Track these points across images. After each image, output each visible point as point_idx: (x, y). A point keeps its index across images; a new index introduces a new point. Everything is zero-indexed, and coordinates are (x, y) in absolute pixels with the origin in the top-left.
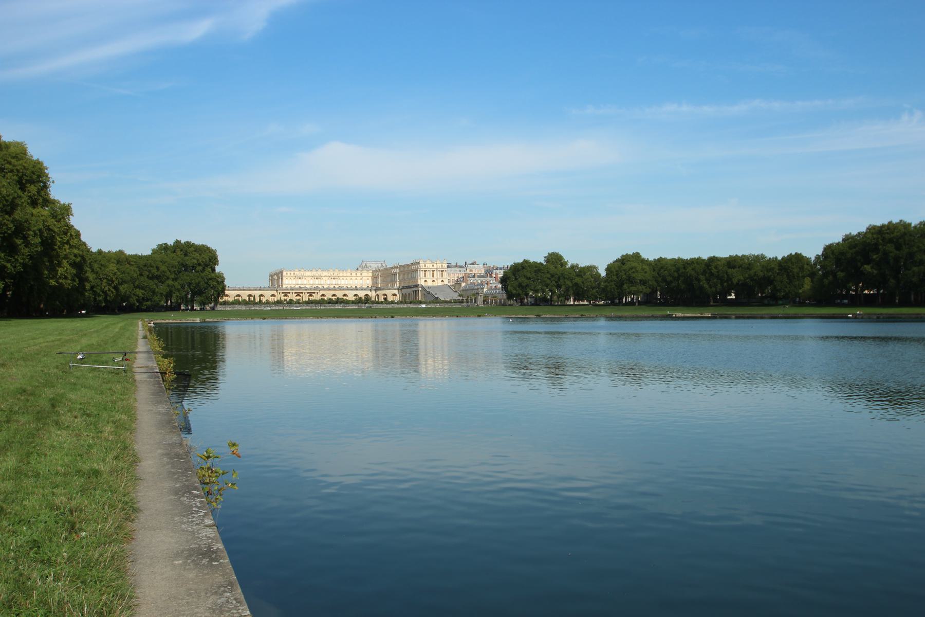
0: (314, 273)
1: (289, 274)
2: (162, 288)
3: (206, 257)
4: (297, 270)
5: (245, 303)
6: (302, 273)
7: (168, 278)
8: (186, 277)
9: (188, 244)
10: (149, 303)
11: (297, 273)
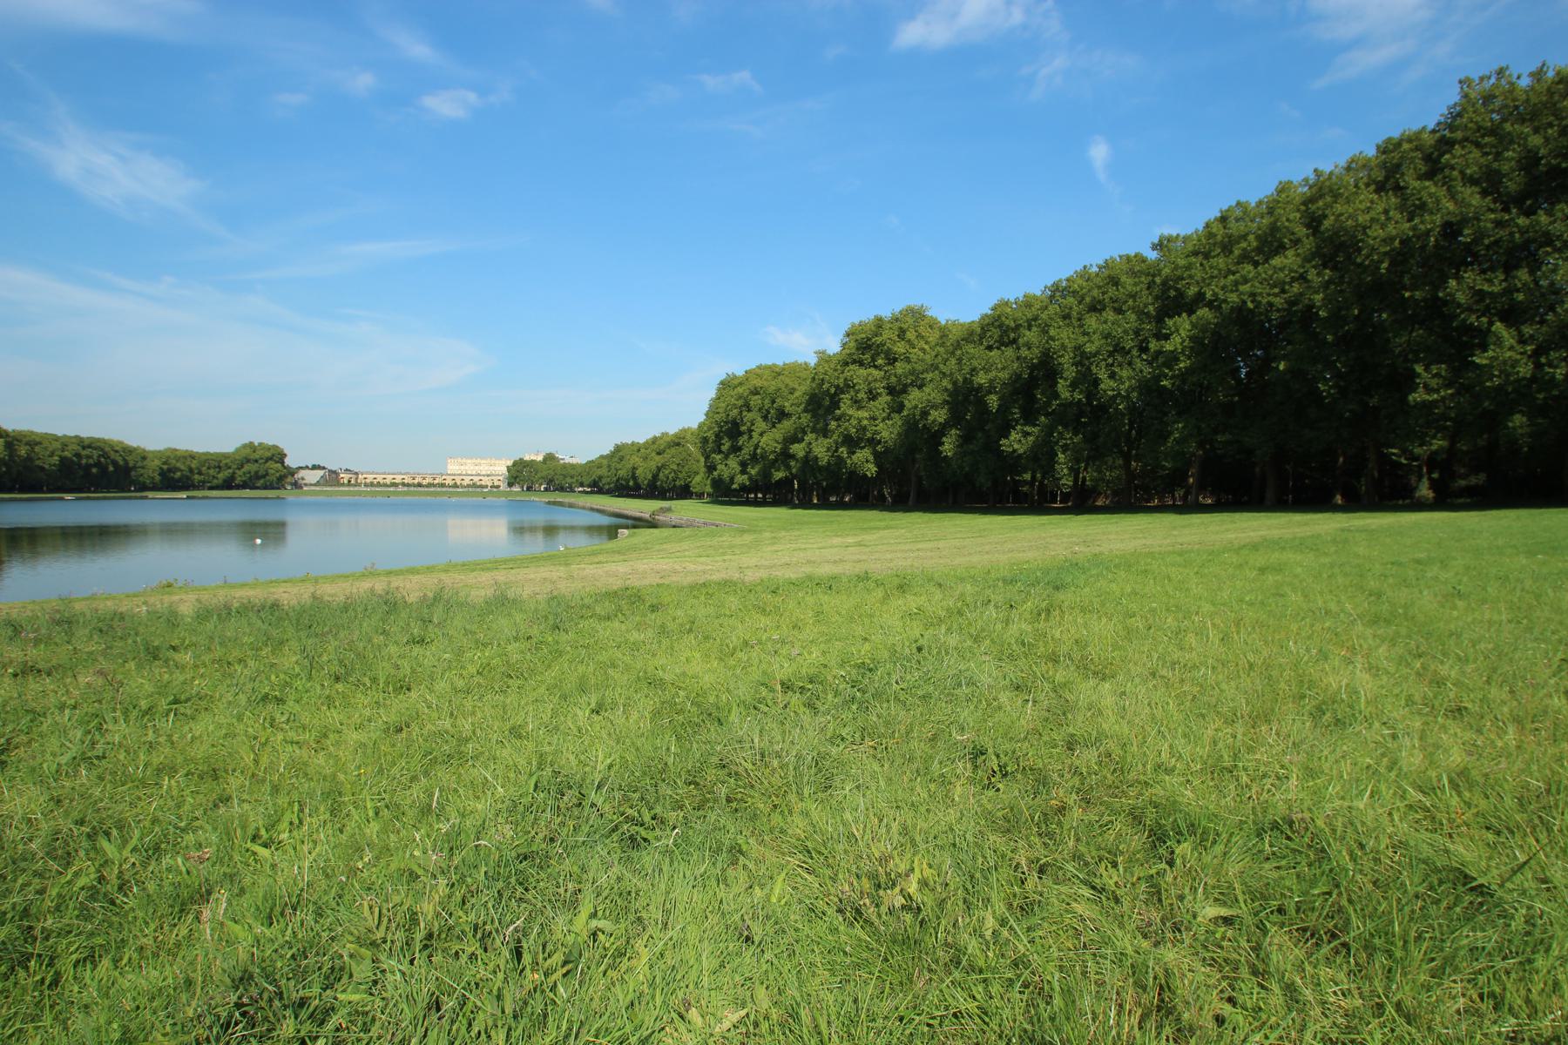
0: (474, 461)
2: (222, 476)
3: (269, 454)
6: (464, 460)
7: (230, 468)
8: (247, 468)
9: (260, 444)
11: (460, 460)
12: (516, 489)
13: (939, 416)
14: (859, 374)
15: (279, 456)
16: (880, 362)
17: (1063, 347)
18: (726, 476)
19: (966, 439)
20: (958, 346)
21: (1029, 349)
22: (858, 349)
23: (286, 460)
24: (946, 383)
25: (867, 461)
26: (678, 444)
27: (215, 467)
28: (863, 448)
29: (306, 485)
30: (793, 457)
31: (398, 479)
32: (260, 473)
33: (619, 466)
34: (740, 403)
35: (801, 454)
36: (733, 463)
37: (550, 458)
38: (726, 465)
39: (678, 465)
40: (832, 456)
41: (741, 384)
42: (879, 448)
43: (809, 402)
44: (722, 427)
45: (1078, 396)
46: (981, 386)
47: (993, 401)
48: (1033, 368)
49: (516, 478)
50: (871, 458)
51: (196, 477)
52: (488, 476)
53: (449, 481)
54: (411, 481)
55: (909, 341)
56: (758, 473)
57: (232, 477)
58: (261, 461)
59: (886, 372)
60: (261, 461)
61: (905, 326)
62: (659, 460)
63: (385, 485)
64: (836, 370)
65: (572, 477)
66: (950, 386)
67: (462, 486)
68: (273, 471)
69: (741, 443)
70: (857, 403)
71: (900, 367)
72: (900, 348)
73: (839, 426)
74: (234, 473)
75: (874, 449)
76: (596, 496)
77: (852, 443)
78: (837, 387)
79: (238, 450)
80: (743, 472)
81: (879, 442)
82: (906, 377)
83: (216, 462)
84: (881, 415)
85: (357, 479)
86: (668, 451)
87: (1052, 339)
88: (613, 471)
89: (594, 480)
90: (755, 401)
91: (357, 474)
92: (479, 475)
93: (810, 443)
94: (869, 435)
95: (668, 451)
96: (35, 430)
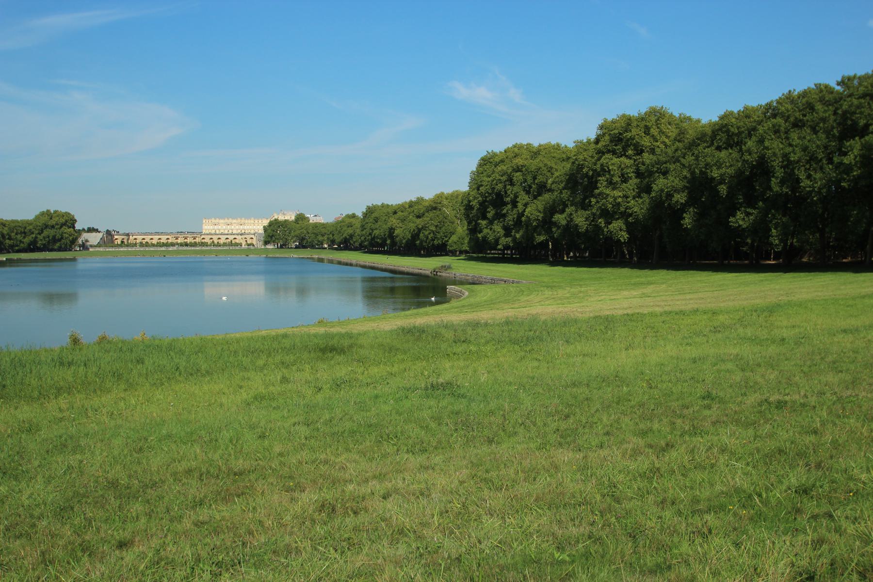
0: (226, 221)
1: (207, 222)
2: (27, 240)
3: (62, 220)
4: (213, 219)
5: (164, 245)
6: (217, 221)
7: (33, 233)
9: (56, 212)
10: (17, 248)
11: (213, 220)
12: (270, 247)
13: (680, 198)
14: (613, 162)
15: (70, 222)
16: (630, 152)
17: (775, 154)
18: (491, 238)
19: (701, 216)
20: (693, 145)
21: (750, 154)
22: (611, 141)
23: (76, 225)
24: (685, 173)
25: (621, 230)
26: (435, 208)
27: (21, 233)
28: (618, 219)
29: (91, 246)
30: (555, 224)
31: (164, 239)
32: (57, 238)
33: (373, 226)
34: (504, 178)
35: (564, 222)
36: (498, 228)
37: (300, 218)
38: (491, 229)
39: (436, 226)
40: (590, 225)
41: (502, 161)
42: (630, 219)
43: (568, 182)
44: (486, 197)
45: (785, 190)
46: (713, 179)
47: (723, 189)
48: (753, 167)
49: (271, 237)
50: (624, 227)
51: (7, 241)
52: (241, 235)
53: (207, 240)
54: (174, 241)
55: (653, 136)
56: (522, 237)
57: (34, 242)
58: (56, 227)
59: (635, 161)
60: (56, 227)
61: (649, 124)
62: (420, 222)
63: (153, 245)
64: (592, 157)
65: (323, 235)
66: (688, 175)
67: (219, 245)
68: (67, 236)
69: (504, 211)
70: (611, 183)
71: (647, 157)
72: (646, 142)
73: (598, 202)
74: (36, 237)
75: (626, 220)
76: (367, 254)
77: (608, 215)
78: (595, 171)
79: (37, 218)
80: (507, 235)
81: (630, 215)
82: (653, 166)
83: (21, 228)
84: (631, 194)
85: (128, 239)
86: (427, 214)
87: (767, 148)
88: (367, 231)
89: (345, 238)
90: (518, 177)
91: (128, 235)
92: (232, 234)
93: (571, 214)
94: (622, 209)
95: (427, 214)
96: (8, 219)
